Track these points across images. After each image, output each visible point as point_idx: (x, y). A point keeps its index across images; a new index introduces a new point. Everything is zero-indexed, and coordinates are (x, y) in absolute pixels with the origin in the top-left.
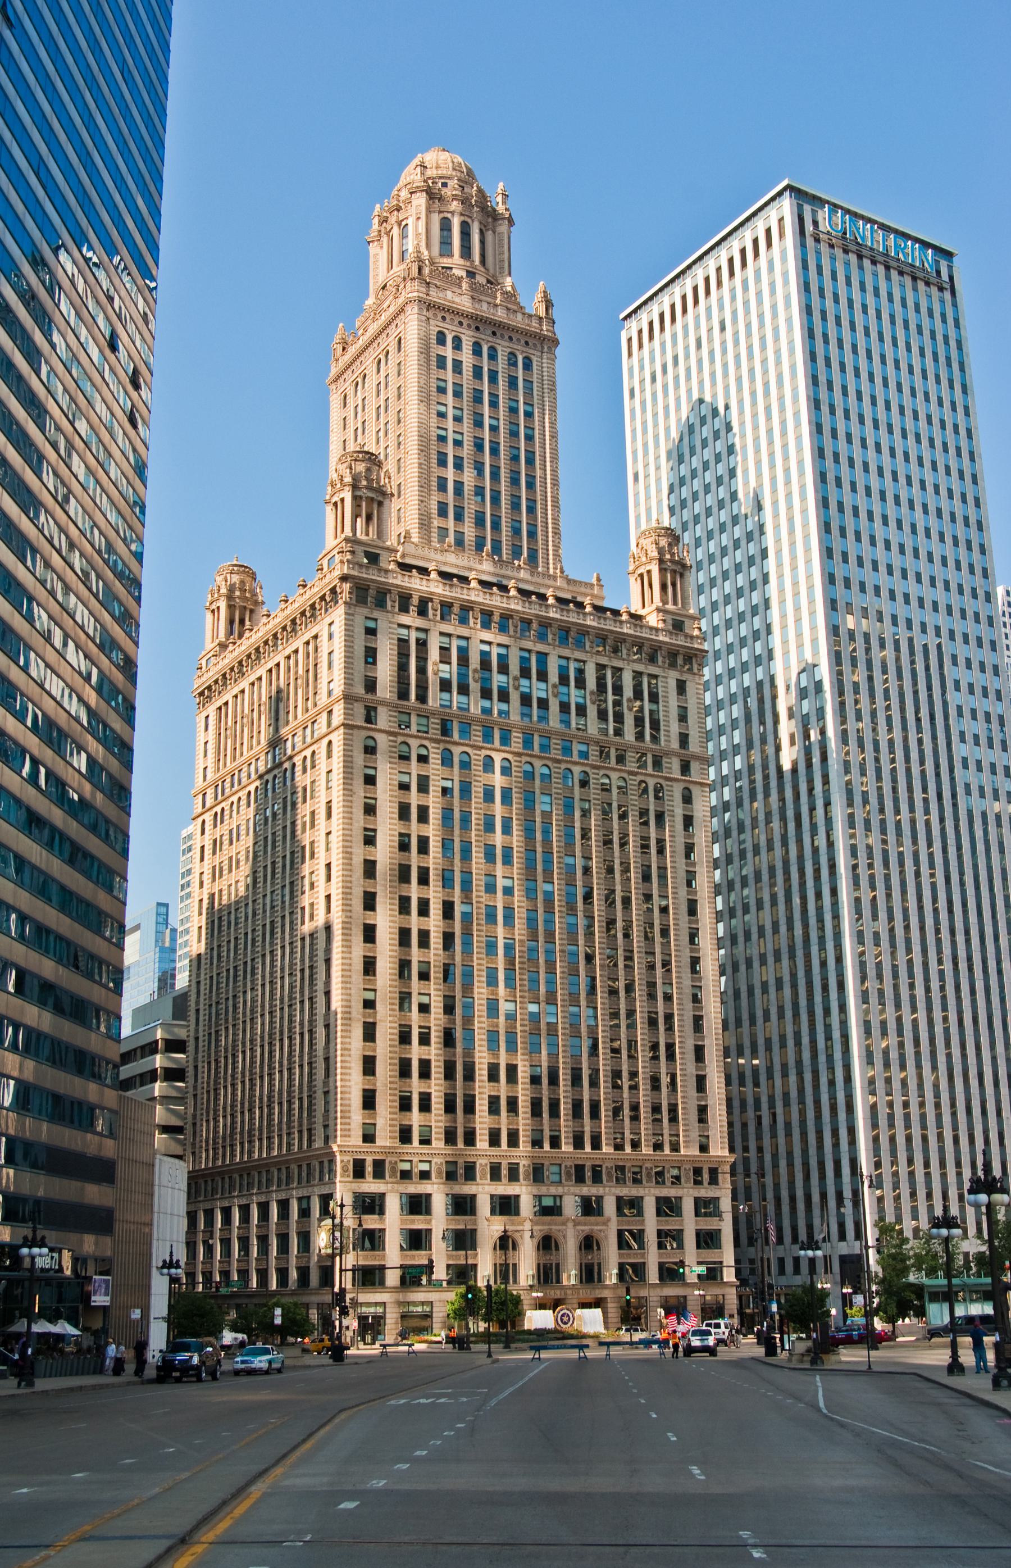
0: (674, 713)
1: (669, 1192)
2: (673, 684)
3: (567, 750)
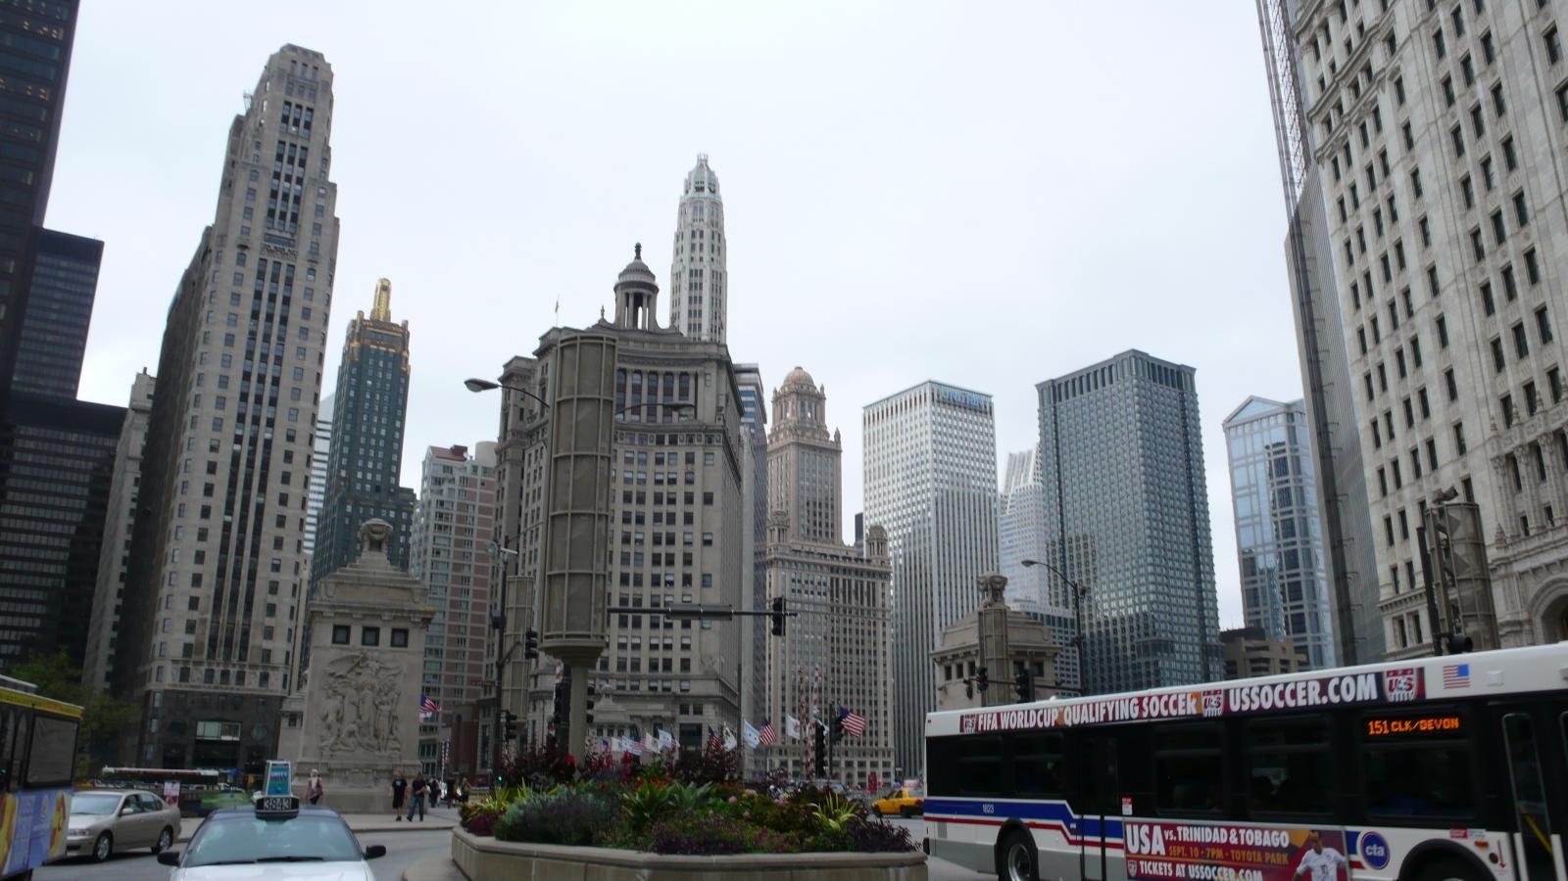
3: (845, 611)
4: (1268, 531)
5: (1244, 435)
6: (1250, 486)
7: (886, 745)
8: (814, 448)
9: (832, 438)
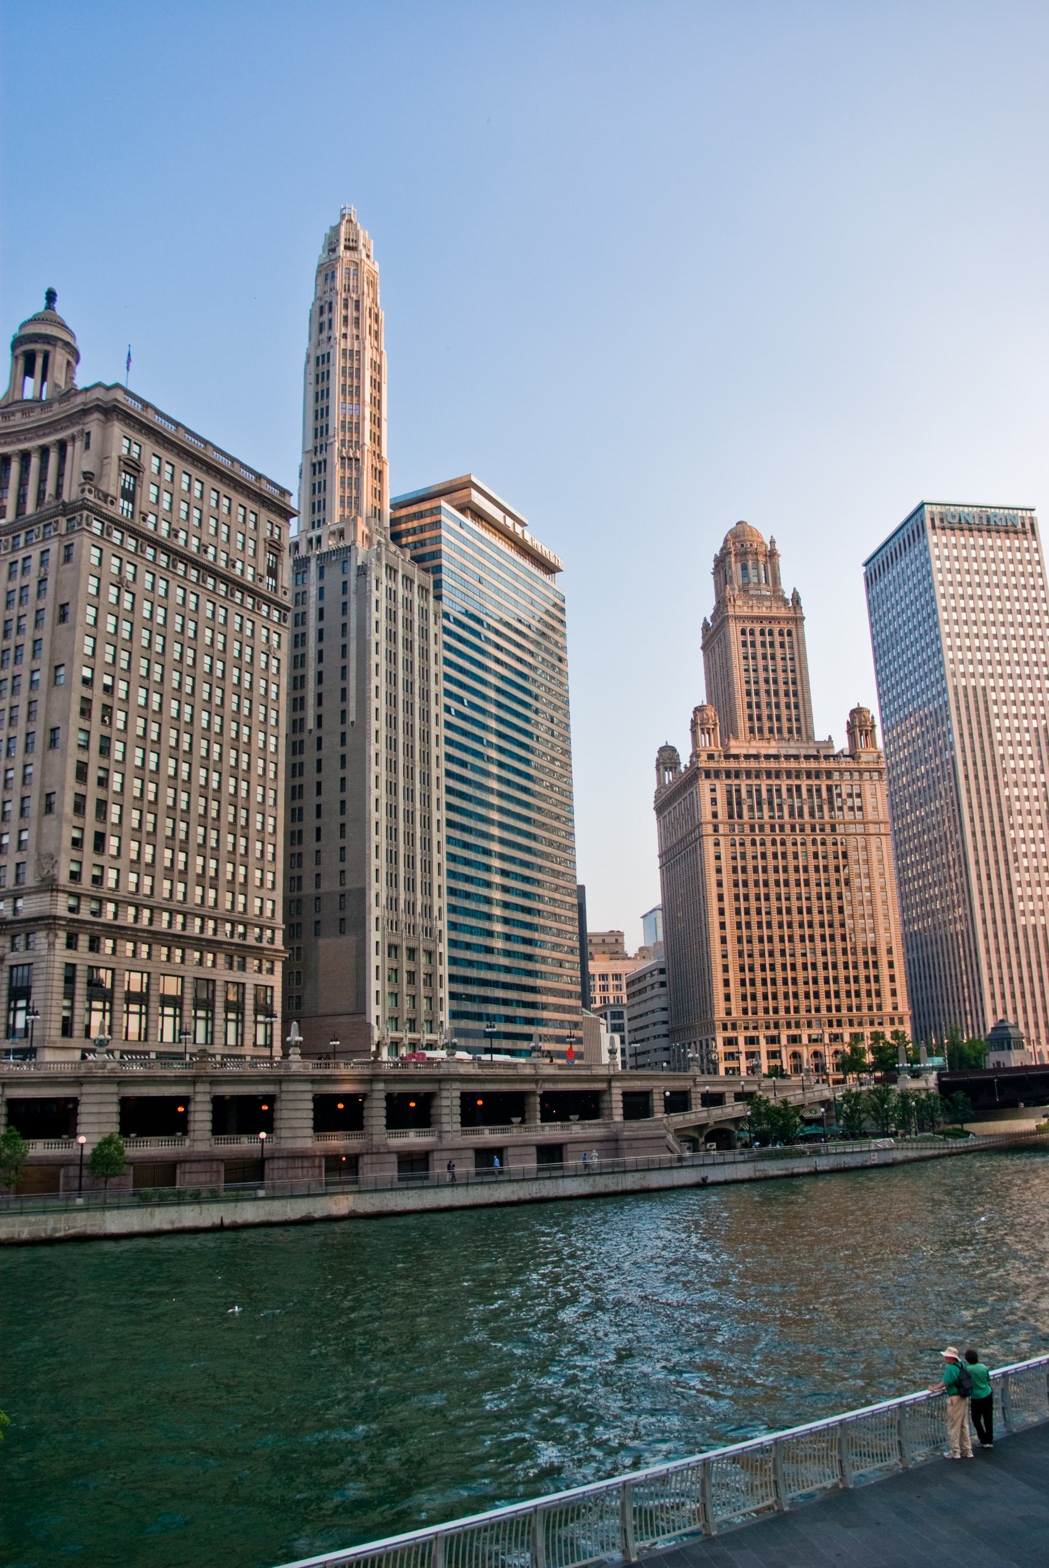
3: (813, 829)
7: (895, 1008)
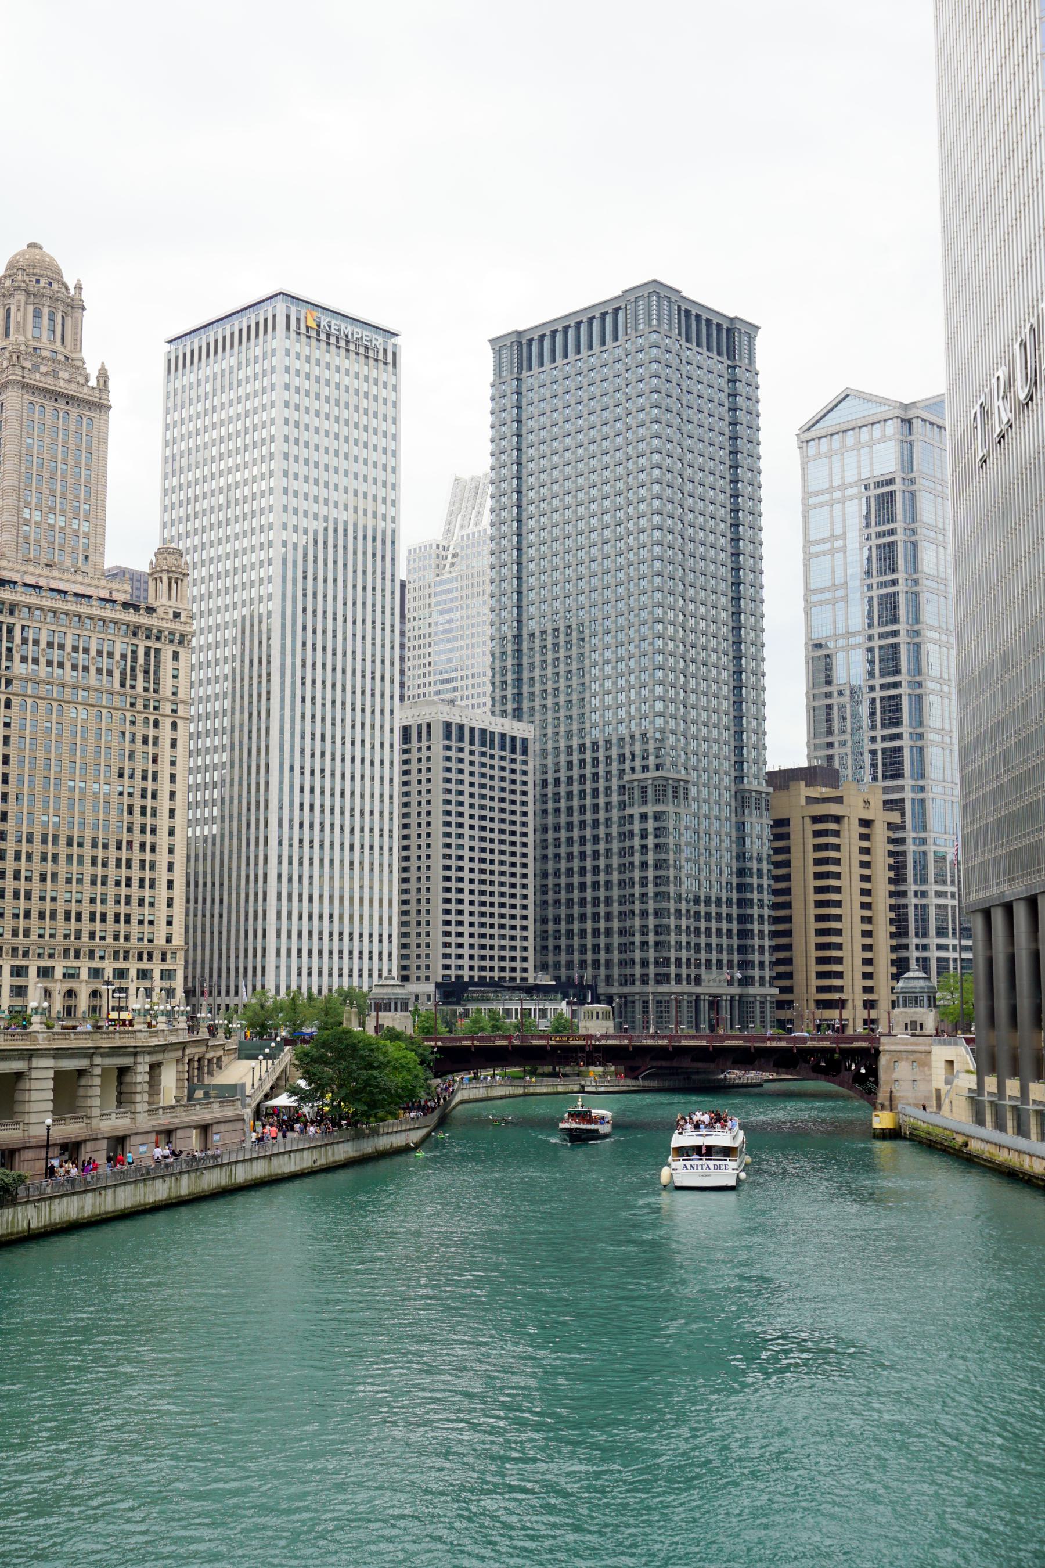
0: (170, 673)
1: (145, 965)
2: (170, 655)
4: (855, 615)
5: (831, 453)
6: (832, 538)
7: (169, 940)
8: (55, 395)
9: (93, 382)
